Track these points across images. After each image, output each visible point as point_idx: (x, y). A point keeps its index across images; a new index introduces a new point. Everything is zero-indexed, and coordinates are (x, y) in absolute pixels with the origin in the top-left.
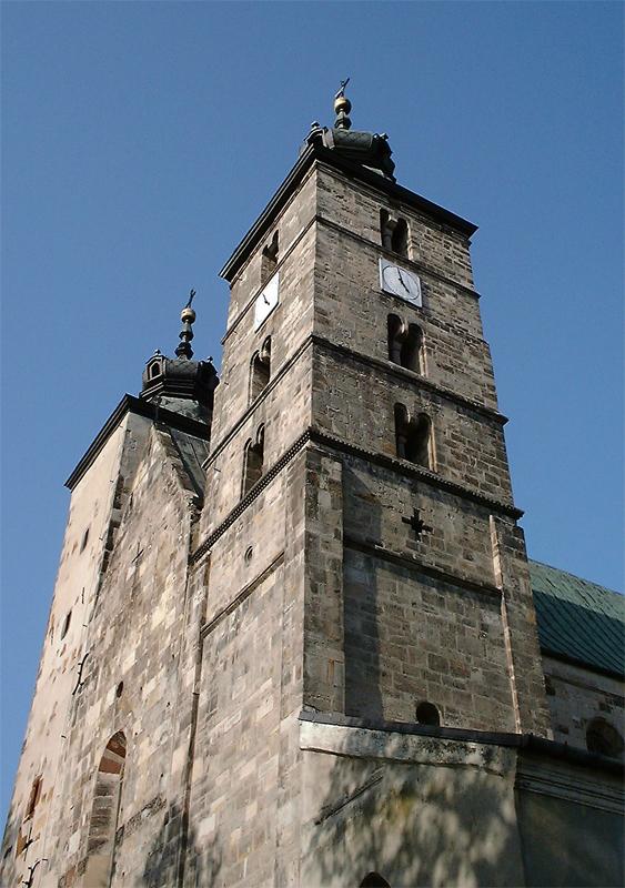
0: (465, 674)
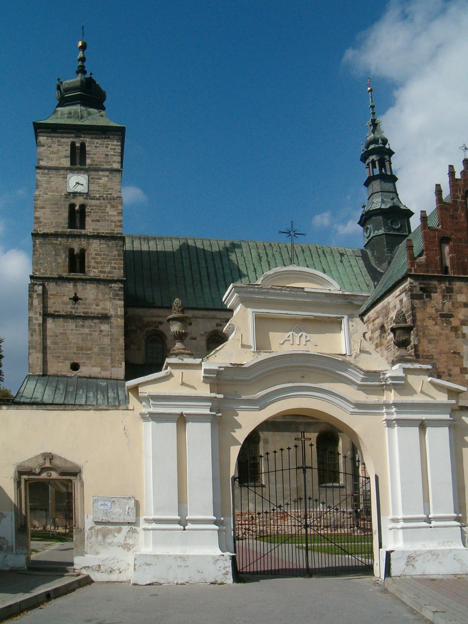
0: (91, 349)
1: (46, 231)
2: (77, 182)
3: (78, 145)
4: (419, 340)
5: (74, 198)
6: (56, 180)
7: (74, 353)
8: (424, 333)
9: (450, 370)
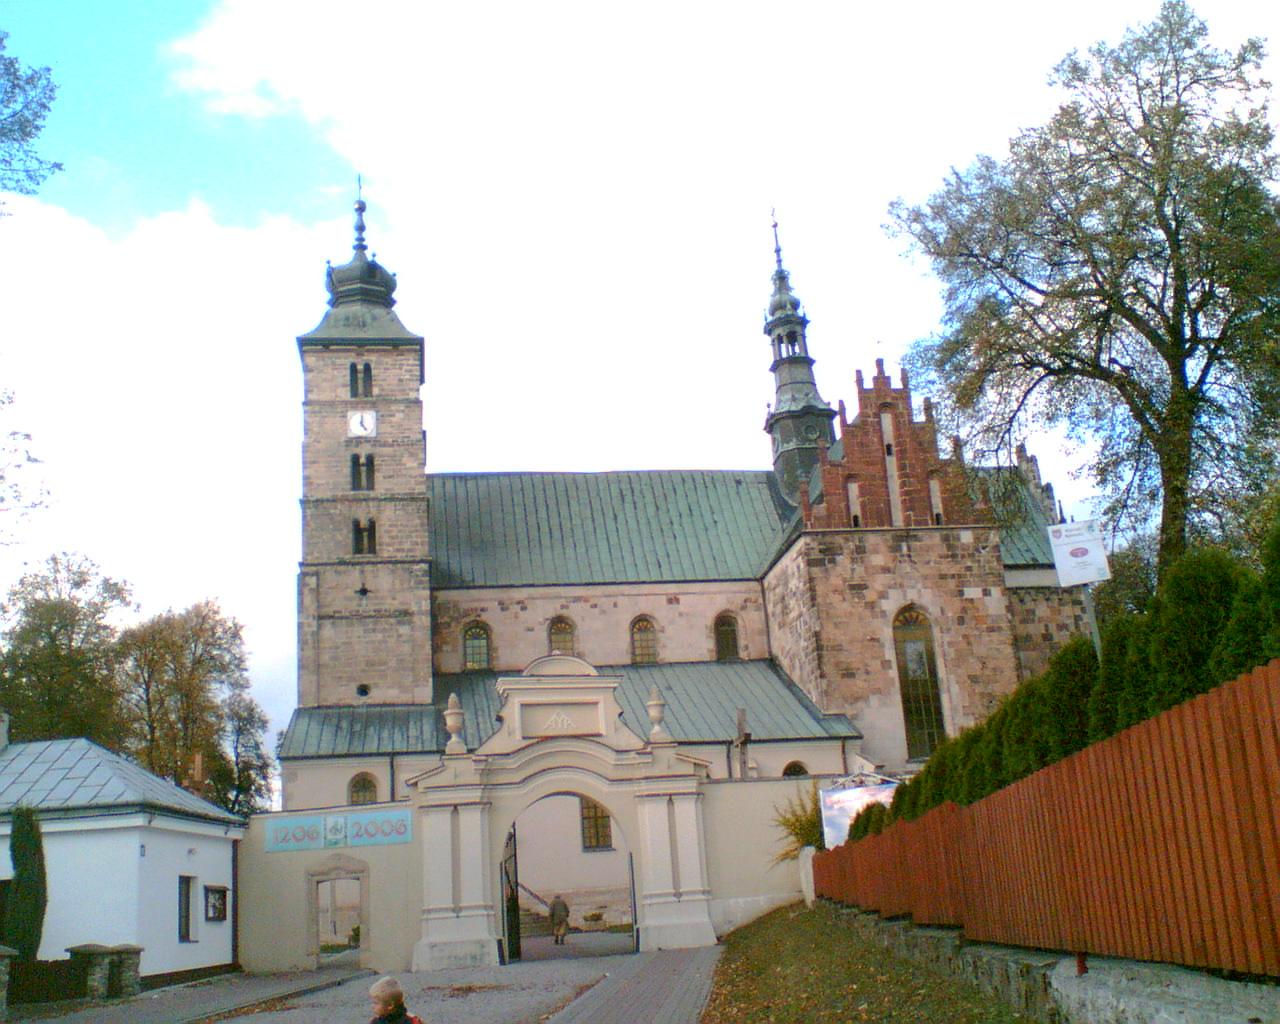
1: (319, 495)
2: (361, 423)
3: (360, 367)
4: (821, 624)
5: (357, 446)
6: (332, 423)
7: (363, 671)
8: (828, 614)
9: (866, 665)
